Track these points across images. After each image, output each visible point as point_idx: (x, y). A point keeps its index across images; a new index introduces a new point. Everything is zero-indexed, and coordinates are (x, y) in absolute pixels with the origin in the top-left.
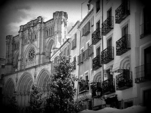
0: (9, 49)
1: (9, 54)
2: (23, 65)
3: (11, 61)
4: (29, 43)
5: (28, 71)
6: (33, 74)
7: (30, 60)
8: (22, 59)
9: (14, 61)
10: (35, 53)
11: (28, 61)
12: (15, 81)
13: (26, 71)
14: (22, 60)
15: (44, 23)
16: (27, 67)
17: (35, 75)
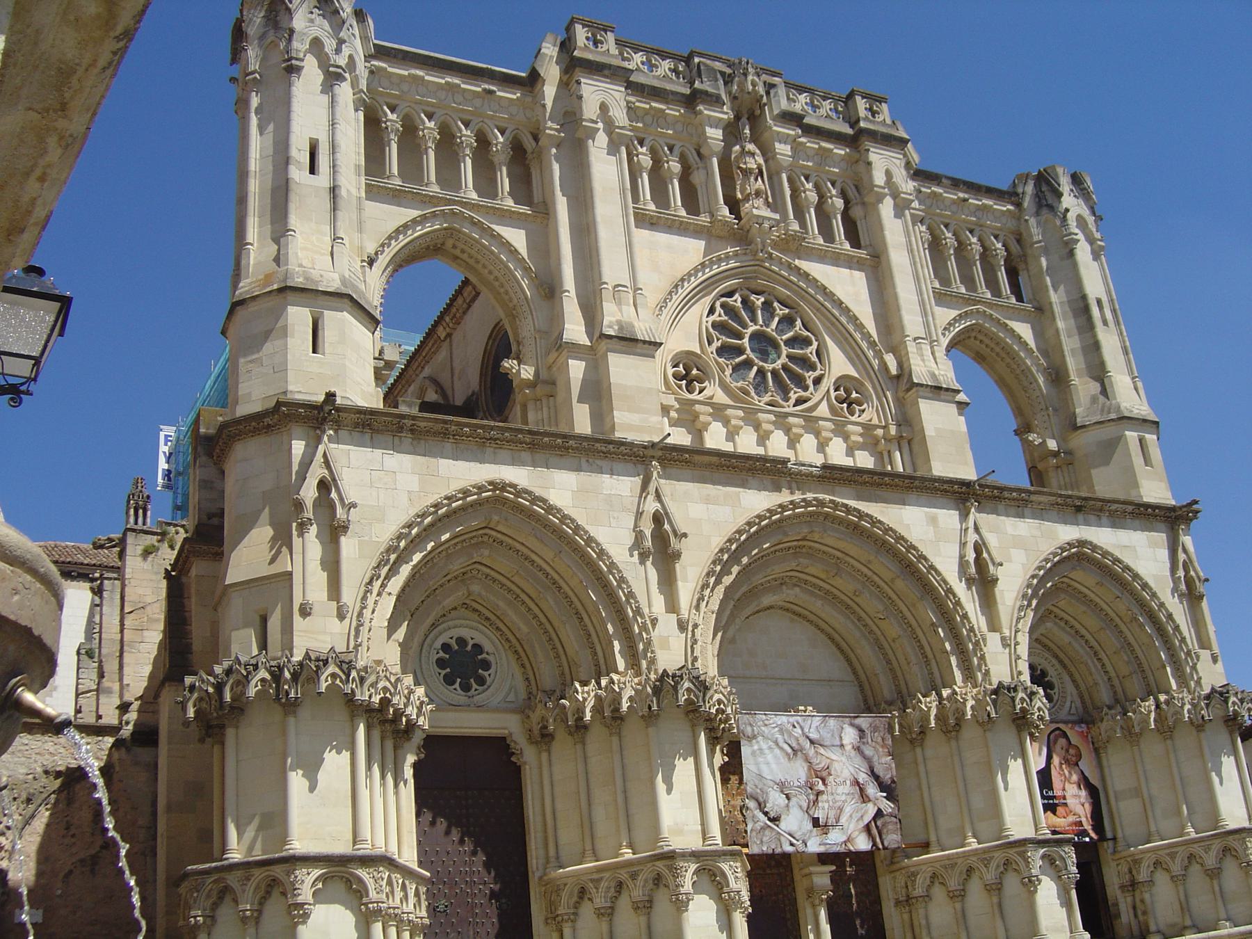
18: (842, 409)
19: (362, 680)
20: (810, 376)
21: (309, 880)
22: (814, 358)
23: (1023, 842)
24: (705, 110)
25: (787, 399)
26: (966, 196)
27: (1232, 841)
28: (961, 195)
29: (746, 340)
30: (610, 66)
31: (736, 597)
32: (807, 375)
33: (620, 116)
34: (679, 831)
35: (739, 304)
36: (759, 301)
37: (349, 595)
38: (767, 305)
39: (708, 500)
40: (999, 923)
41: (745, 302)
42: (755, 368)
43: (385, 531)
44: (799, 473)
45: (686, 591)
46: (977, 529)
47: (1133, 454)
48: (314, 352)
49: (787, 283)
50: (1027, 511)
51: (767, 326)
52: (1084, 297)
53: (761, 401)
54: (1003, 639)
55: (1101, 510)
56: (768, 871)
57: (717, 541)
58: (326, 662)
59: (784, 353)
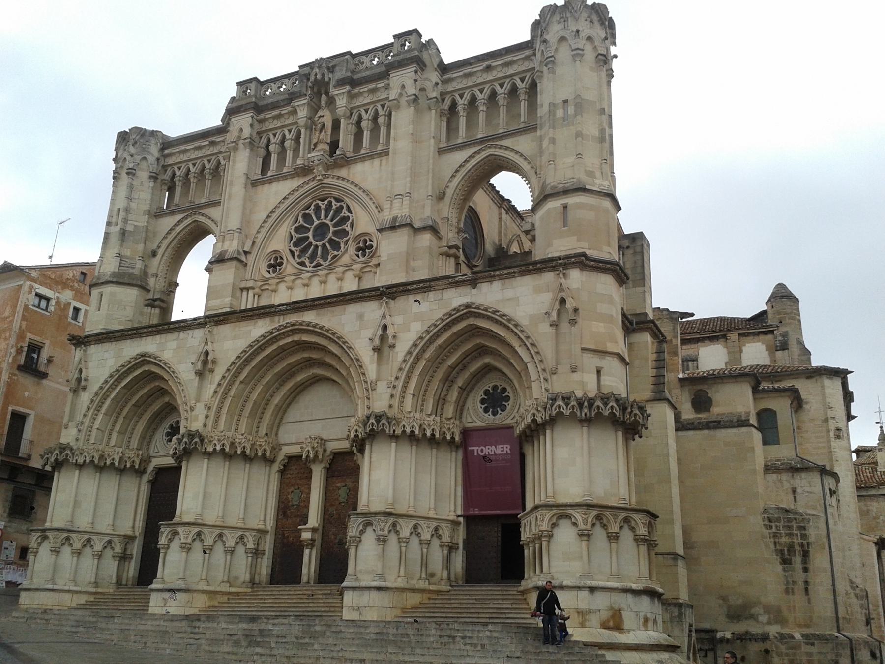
0: (129, 198)
1: (129, 228)
2: (250, 284)
3: (139, 265)
4: (305, 170)
5: (310, 317)
6: (368, 333)
7: (302, 264)
8: (246, 253)
9: (152, 271)
11: (290, 267)
13: (293, 318)
14: (243, 258)
15: (444, 69)
16: (282, 296)
17: (383, 338)
23: (376, 514)
24: (295, 103)
28: (485, 64)
29: (310, 234)
30: (242, 106)
33: (247, 132)
36: (323, 205)
39: (235, 338)
41: (318, 208)
43: (95, 388)
44: (281, 311)
46: (384, 317)
50: (431, 295)
51: (326, 217)
55: (492, 277)
57: (233, 359)
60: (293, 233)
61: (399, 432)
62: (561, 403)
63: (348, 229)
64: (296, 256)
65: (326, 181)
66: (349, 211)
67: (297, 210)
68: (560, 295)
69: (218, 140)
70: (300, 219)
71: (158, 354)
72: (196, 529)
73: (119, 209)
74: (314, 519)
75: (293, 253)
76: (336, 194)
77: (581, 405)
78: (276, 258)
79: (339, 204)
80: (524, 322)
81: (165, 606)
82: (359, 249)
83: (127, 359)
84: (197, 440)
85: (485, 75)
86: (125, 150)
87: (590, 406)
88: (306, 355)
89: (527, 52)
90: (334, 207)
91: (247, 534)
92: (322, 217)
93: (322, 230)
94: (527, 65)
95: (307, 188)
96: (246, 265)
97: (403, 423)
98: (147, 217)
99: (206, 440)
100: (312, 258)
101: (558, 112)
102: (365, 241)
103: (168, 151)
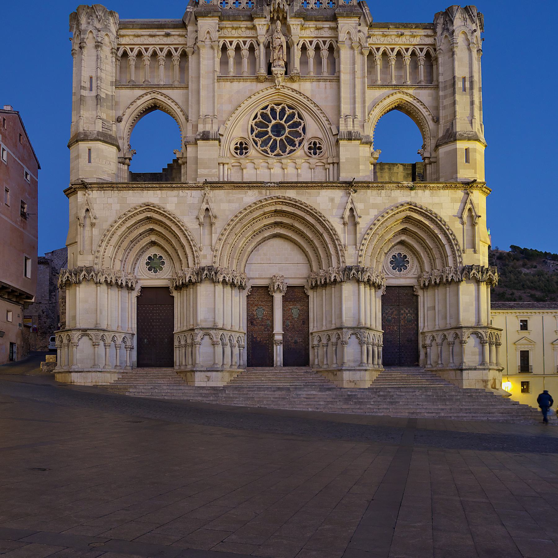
1: (103, 96)
10: (300, 129)
12: (189, 222)
18: (310, 153)
19: (96, 275)
20: (297, 141)
21: (76, 336)
22: (301, 131)
25: (284, 152)
26: (403, 31)
27: (458, 331)
29: (269, 129)
31: (246, 236)
32: (296, 139)
34: (205, 321)
35: (269, 113)
37: (95, 248)
38: (283, 111)
40: (334, 356)
41: (273, 110)
42: (272, 140)
43: (106, 226)
45: (215, 237)
47: (458, 157)
48: (90, 162)
49: (292, 98)
51: (281, 119)
52: (454, 77)
53: (271, 155)
54: (356, 248)
56: (264, 332)
58: (82, 271)
59: (287, 132)
60: (254, 126)
61: (366, 280)
62: (475, 271)
63: (301, 131)
64: (259, 144)
65: (282, 90)
66: (300, 117)
67: (258, 110)
68: (468, 206)
69: (173, 33)
70: (259, 116)
71: (162, 205)
72: (221, 332)
73: (91, 78)
74: (278, 328)
75: (256, 144)
76: (290, 102)
77: (482, 273)
78: (241, 144)
79: (291, 111)
80: (446, 220)
81: (208, 381)
82: (310, 148)
83: (132, 206)
84: (213, 273)
85: (397, 39)
86: (89, 23)
87: (487, 273)
88: (278, 219)
89: (429, 32)
90: (288, 113)
91: (241, 335)
92: (278, 118)
93: (278, 130)
94: (429, 41)
95: (266, 92)
96: (220, 145)
97: (368, 274)
98: (114, 87)
99: (219, 273)
100: (273, 149)
101: (459, 83)
102: (315, 144)
103: (123, 32)
